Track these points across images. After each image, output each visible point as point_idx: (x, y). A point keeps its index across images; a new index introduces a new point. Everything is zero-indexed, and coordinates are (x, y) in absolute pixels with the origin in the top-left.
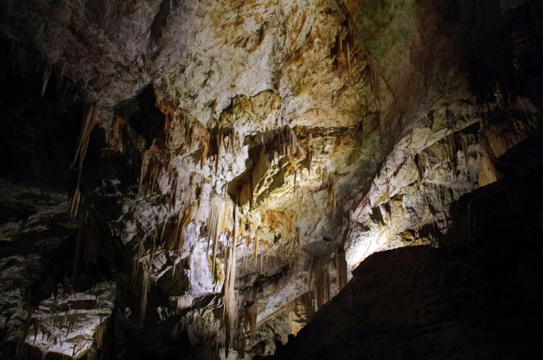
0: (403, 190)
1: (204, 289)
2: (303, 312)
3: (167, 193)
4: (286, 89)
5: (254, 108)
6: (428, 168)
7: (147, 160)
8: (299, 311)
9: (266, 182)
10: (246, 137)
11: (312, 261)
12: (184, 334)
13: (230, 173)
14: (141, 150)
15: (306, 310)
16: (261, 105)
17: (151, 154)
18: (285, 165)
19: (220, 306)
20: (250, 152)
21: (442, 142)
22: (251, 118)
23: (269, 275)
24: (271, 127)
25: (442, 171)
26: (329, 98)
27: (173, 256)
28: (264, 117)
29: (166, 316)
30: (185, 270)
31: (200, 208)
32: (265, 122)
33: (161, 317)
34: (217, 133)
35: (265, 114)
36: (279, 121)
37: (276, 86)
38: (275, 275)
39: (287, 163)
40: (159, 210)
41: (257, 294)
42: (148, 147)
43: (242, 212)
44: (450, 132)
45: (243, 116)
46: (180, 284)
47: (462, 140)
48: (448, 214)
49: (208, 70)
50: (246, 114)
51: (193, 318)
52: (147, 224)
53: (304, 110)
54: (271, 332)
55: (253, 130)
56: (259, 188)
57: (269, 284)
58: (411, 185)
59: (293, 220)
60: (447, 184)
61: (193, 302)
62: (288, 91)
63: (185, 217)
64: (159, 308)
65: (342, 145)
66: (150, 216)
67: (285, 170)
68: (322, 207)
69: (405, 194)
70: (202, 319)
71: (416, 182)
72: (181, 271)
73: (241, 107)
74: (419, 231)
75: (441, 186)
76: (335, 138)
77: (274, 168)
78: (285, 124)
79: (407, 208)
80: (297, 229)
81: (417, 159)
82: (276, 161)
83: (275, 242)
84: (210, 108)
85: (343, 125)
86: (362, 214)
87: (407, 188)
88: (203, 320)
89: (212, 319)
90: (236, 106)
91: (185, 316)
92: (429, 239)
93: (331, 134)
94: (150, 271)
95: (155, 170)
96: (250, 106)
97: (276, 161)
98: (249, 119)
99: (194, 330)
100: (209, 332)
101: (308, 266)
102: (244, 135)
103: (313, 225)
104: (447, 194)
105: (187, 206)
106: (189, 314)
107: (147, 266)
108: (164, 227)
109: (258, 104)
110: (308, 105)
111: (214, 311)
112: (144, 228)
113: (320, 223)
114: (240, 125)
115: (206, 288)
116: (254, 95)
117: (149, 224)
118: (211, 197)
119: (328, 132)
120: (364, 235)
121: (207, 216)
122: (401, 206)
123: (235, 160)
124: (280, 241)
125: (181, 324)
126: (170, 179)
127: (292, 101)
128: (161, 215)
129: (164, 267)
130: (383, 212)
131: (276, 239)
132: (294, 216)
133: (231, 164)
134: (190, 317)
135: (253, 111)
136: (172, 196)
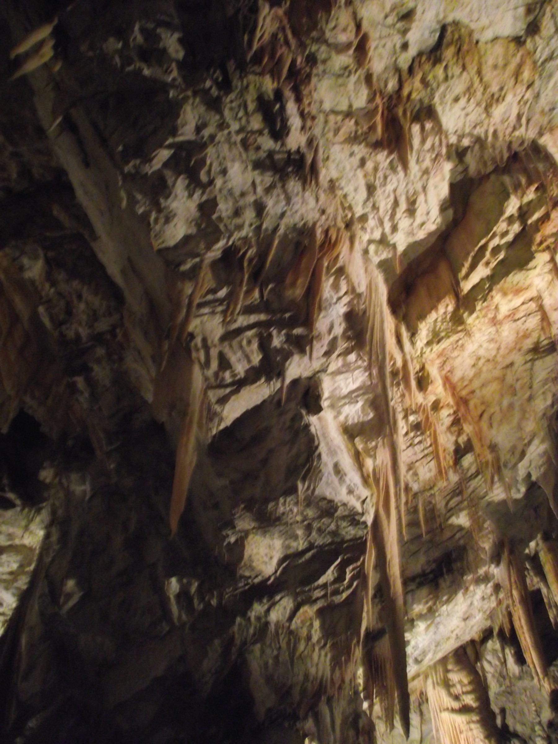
1: (344, 490)
2: (465, 689)
9: (488, 254)
12: (235, 673)
16: (495, 67)
18: (536, 216)
19: (344, 595)
28: (495, 99)
30: (304, 412)
32: (498, 111)
33: (175, 609)
34: (396, 106)
35: (501, 89)
36: (524, 120)
40: (268, 190)
46: (283, 458)
51: (267, 624)
52: (230, 212)
56: (473, 267)
64: (174, 580)
66: (243, 194)
72: (289, 415)
73: (459, 50)
78: (531, 134)
82: (512, 206)
89: (316, 635)
90: (449, 44)
96: (476, 58)
97: (512, 206)
99: (266, 664)
100: (306, 676)
103: (520, 448)
106: (258, 609)
108: (276, 242)
109: (490, 62)
111: (320, 613)
112: (220, 219)
113: (536, 442)
114: (449, 98)
117: (237, 213)
124: (468, 460)
125: (232, 639)
128: (274, 205)
131: (460, 452)
132: (486, 417)
133: (415, 193)
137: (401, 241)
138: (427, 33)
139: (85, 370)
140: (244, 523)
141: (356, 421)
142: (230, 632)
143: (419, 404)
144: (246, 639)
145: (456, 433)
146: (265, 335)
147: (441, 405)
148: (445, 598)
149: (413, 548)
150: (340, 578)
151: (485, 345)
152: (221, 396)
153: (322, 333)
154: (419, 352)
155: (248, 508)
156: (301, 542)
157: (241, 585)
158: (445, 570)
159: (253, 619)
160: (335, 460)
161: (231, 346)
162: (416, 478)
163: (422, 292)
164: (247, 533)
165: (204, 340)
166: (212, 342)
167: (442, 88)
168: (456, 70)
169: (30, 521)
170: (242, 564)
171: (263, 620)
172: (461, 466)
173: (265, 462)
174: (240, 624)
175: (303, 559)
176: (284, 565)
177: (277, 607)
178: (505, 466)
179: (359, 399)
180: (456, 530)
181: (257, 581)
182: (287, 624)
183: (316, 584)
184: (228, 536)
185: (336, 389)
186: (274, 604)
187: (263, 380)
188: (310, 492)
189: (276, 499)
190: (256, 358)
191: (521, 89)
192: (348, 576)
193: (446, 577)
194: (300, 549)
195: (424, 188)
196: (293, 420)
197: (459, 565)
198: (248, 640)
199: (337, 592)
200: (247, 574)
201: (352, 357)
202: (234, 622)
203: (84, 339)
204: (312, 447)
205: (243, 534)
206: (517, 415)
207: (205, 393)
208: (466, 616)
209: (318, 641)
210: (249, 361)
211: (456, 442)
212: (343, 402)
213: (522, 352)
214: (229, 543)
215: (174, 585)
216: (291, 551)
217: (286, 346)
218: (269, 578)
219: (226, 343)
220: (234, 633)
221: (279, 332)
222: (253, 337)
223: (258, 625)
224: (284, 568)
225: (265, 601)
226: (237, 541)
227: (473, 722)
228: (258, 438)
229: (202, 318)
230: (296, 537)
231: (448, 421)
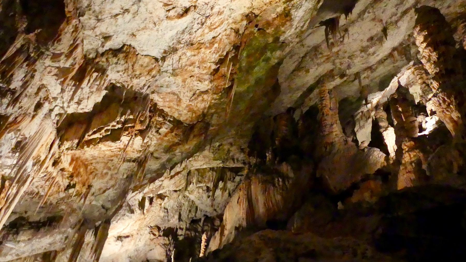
0: (167, 192)
3: (14, 89)
4: (169, 65)
5: (136, 65)
6: (193, 183)
7: (20, 43)
9: (103, 131)
10: (111, 83)
11: (82, 221)
13: (76, 106)
14: (19, 30)
16: (142, 66)
17: (26, 41)
20: (105, 97)
21: (212, 169)
22: (127, 71)
23: (31, 220)
24: (136, 88)
25: (201, 191)
26: (192, 93)
31: (32, 122)
32: (135, 81)
34: (90, 64)
35: (140, 74)
36: (146, 88)
37: (164, 59)
38: (39, 222)
39: (133, 125)
41: (11, 236)
42: (28, 31)
43: (59, 147)
44: (221, 165)
45: (122, 65)
47: (227, 174)
48: (188, 225)
49: (127, 8)
50: (126, 65)
53: (169, 90)
55: (120, 81)
56: (94, 133)
58: (176, 191)
59: (91, 177)
60: (197, 202)
62: (170, 68)
63: (15, 122)
65: (173, 134)
67: (126, 129)
68: (121, 177)
69: (168, 197)
71: (180, 190)
73: (127, 56)
74: (164, 230)
75: (193, 201)
76: (172, 126)
77: (118, 123)
78: (148, 92)
79: (165, 208)
80: (90, 187)
81: (189, 173)
83: (65, 190)
84: (103, 40)
85: (182, 119)
86: (134, 198)
87: (172, 192)
90: (123, 52)
92: (169, 239)
93: (169, 121)
95: (22, 58)
98: (125, 70)
101: (76, 225)
102: (110, 80)
103: (104, 189)
104: (194, 209)
105: (23, 112)
110: (175, 88)
116: (142, 54)
118: (45, 117)
119: (169, 118)
120: (127, 216)
121: (32, 134)
122: (161, 204)
123: (88, 97)
124: (71, 191)
126: (25, 77)
127: (167, 79)
130: (147, 203)
131: (69, 187)
132: (94, 174)
133: (83, 98)
135: (133, 66)
136: (17, 95)
137: (70, 111)
138: (116, 44)
148: (39, 236)
154: (61, 151)
163: (73, 130)
167: (114, 65)
168: (122, 62)
172: (68, 191)
191: (148, 77)
195: (88, 97)
206: (109, 177)
211: (70, 183)
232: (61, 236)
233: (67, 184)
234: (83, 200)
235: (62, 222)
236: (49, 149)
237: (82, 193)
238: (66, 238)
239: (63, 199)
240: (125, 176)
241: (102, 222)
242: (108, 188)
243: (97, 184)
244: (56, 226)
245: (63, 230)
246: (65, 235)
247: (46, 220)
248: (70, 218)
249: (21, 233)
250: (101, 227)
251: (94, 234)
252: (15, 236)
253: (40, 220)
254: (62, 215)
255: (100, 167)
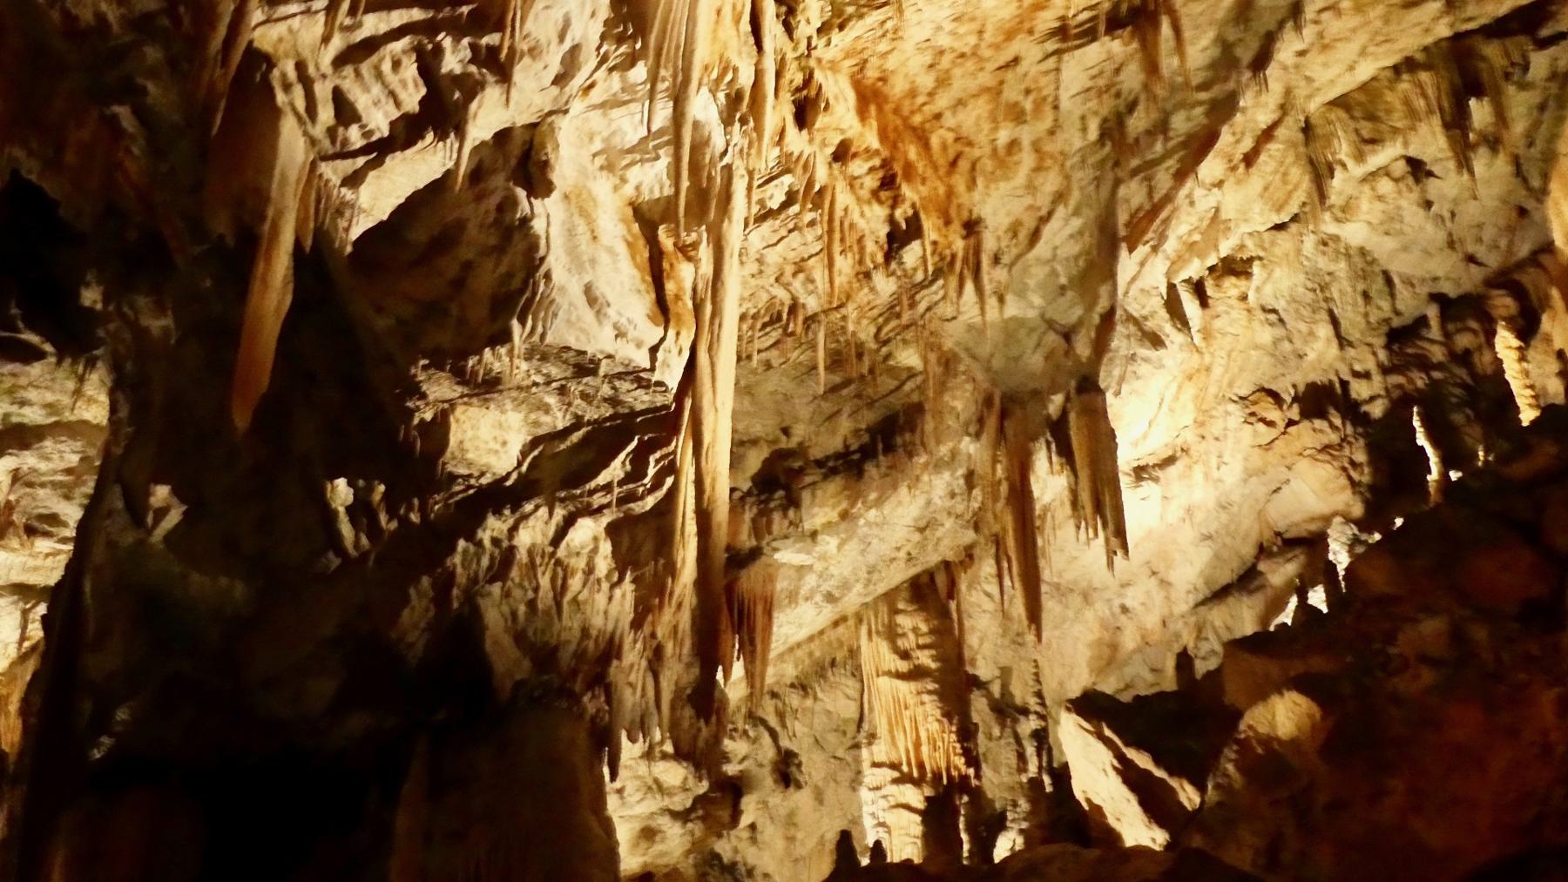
0: (1249, 243)
1: (609, 332)
2: (921, 641)
6: (1344, 165)
8: (904, 635)
12: (460, 630)
15: (932, 632)
19: (650, 502)
21: (1407, 66)
23: (816, 453)
25: (1385, 186)
27: (466, 76)
29: (374, 530)
30: (521, 193)
33: (346, 529)
41: (777, 516)
43: (789, 29)
44: (1443, 30)
46: (486, 279)
47: (1484, 59)
48: (1383, 355)
51: (512, 549)
54: (766, 739)
57: (825, 477)
58: (1279, 227)
60: (1383, 248)
61: (524, 454)
64: (341, 483)
68: (1078, 143)
69: (1260, 258)
70: (558, 563)
71: (1295, 218)
72: (493, 201)
74: (1295, 399)
75: (1363, 252)
79: (1264, 310)
80: (972, 227)
81: (1307, 129)
83: (890, 256)
86: (1139, 284)
87: (1266, 236)
88: (562, 572)
89: (604, 564)
91: (471, 537)
92: (1332, 426)
94: (319, 131)
99: (514, 614)
100: (585, 632)
103: (1030, 223)
104: (1379, 284)
106: (494, 526)
107: (298, 93)
111: (612, 530)
115: (620, 334)
120: (1146, 360)
122: (1244, 298)
124: (912, 254)
129: (406, 133)
130: (1190, 305)
131: (898, 238)
132: (964, 165)
134: (496, 542)
139: (131, 92)
140: (440, 388)
141: (657, 195)
142: (448, 563)
143: (796, 154)
144: (476, 573)
145: (890, 202)
146: (430, 47)
147: (853, 150)
149: (828, 407)
150: (636, 474)
151: (948, 26)
152: (350, 171)
153: (543, 41)
155: (437, 364)
156: (560, 415)
157: (457, 488)
158: (880, 446)
159: (487, 543)
160: (587, 279)
161: (358, 74)
162: (811, 287)
164: (452, 404)
165: (300, 66)
166: (317, 68)
169: (81, 380)
170: (448, 454)
171: (505, 544)
172: (901, 263)
173: (459, 284)
174: (465, 551)
175: (568, 443)
176: (536, 453)
177: (531, 521)
178: (996, 260)
179: (661, 152)
180: (904, 376)
181: (484, 481)
182: (551, 549)
183: (593, 484)
184: (418, 409)
185: (614, 133)
186: (526, 517)
187: (430, 136)
188: (536, 338)
189: (479, 352)
190: (413, 97)
192: (651, 471)
193: (881, 458)
194: (560, 426)
196: (500, 208)
197: (907, 436)
198: (481, 575)
199: (631, 497)
200: (463, 471)
201: (640, 72)
202: (453, 549)
203: (116, 28)
204: (533, 259)
205: (446, 406)
206: (1027, 159)
207: (313, 165)
208: (922, 524)
209: (608, 576)
210: (398, 104)
211: (891, 220)
212: (628, 159)
213: (1037, 35)
214: (422, 421)
215: (341, 492)
216: (541, 431)
217: (473, 69)
218: (509, 474)
219: (348, 70)
220: (454, 566)
221: (457, 40)
222: (404, 52)
223: (497, 552)
224: (535, 458)
225: (507, 512)
226: (434, 419)
227: (930, 692)
228: (447, 239)
229: (289, 21)
230: (547, 409)
231: (871, 182)
232: (947, 475)
233: (884, 230)
234: (969, 287)
235: (929, 425)
236: (752, 40)
237: (954, 256)
238: (970, 478)
239: (892, 311)
240: (1093, 134)
241: (1068, 399)
242: (1044, 212)
243: (998, 205)
244: (913, 443)
245: (944, 450)
246: (961, 472)
247: (866, 438)
248: (947, 398)
249: (806, 496)
250: (1072, 417)
251: (1060, 453)
252: (791, 513)
253: (846, 447)
254: (915, 398)
255: (973, 118)
